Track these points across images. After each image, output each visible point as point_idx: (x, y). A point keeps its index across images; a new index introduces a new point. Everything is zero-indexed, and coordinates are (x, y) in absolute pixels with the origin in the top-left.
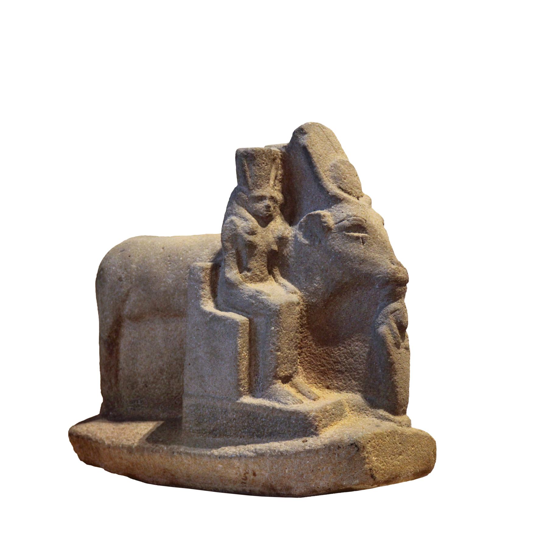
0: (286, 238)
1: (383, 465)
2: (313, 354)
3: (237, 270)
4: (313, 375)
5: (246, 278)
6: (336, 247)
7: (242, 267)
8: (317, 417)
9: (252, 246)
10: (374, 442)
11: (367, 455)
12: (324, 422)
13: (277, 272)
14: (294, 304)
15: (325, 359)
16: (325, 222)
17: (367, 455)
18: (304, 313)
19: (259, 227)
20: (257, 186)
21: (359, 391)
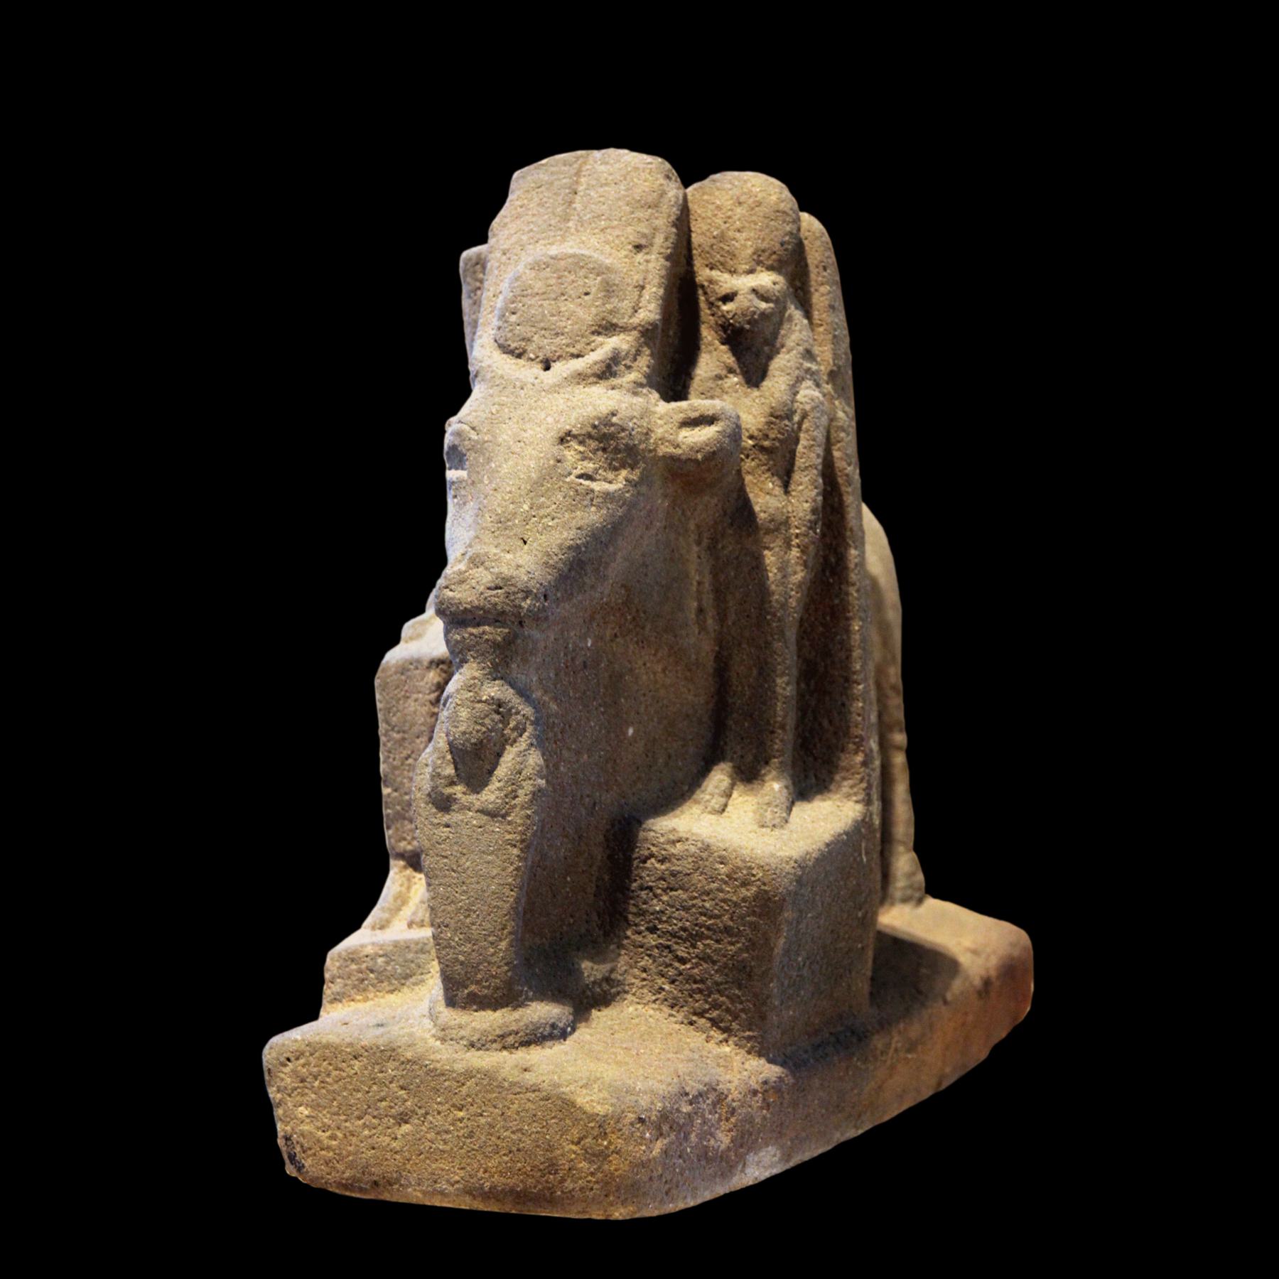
1: (333, 1137)
10: (303, 1066)
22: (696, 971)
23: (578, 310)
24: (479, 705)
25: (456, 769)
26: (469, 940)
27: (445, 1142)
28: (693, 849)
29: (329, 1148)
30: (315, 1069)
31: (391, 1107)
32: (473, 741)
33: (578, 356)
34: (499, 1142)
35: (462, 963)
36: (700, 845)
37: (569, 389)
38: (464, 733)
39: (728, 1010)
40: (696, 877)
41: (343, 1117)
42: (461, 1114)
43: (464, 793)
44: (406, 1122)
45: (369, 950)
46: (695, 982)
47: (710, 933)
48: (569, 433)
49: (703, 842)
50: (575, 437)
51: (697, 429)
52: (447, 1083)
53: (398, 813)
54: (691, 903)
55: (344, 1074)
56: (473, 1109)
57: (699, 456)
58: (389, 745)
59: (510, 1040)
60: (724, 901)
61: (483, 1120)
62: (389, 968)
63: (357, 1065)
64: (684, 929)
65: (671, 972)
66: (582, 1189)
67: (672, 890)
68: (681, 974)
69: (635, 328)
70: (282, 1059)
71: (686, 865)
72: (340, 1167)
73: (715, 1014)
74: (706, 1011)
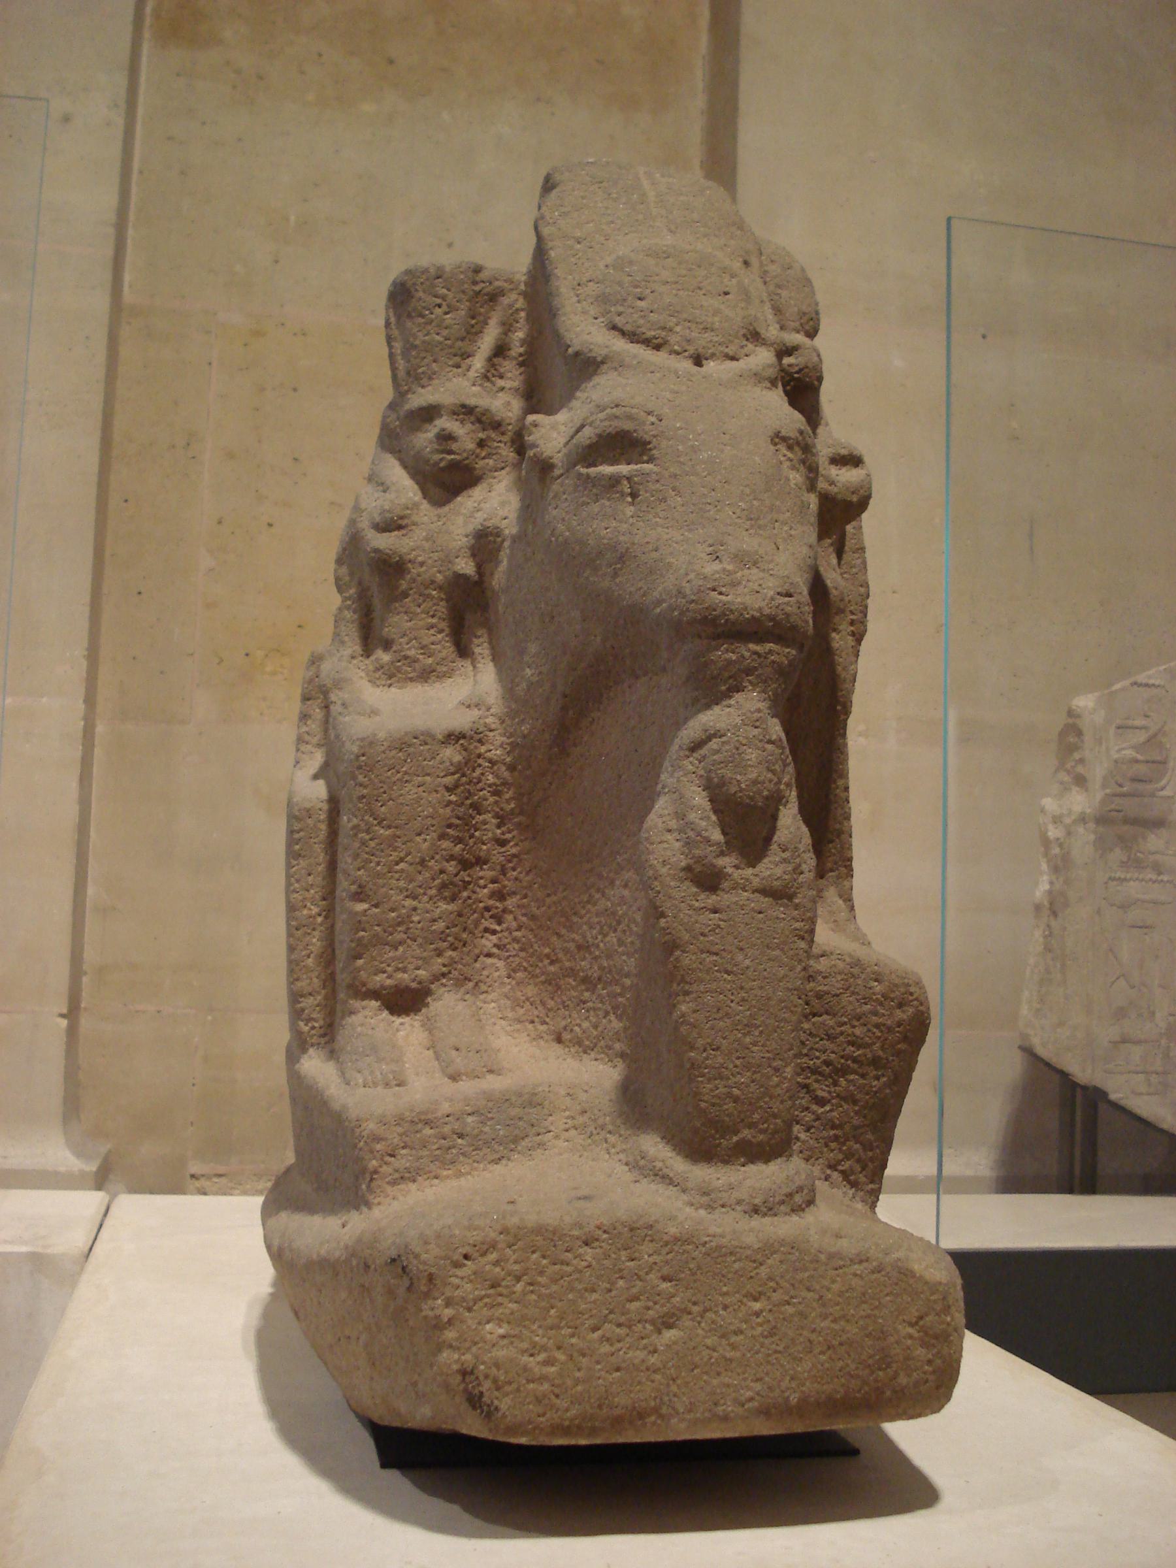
0: (497, 532)
1: (548, 1362)
2: (533, 918)
3: (358, 649)
4: (531, 990)
5: (377, 669)
6: (561, 527)
7: (370, 637)
8: (378, 1139)
9: (390, 569)
10: (496, 1263)
11: (448, 1312)
12: (404, 1160)
13: (481, 648)
14: (433, 737)
15: (559, 935)
16: (534, 446)
17: (448, 1312)
18: (506, 774)
19: (425, 505)
20: (418, 378)
21: (622, 1055)
22: (835, 1114)
23: (722, 307)
24: (769, 747)
25: (724, 833)
26: (747, 1067)
27: (734, 1347)
28: (841, 965)
29: (543, 1378)
30: (516, 1267)
31: (648, 1308)
32: (765, 793)
33: (733, 358)
34: (813, 1337)
35: (736, 1100)
36: (848, 960)
37: (749, 388)
38: (755, 782)
39: (858, 1161)
40: (845, 998)
41: (566, 1331)
42: (757, 1306)
43: (737, 867)
44: (670, 1326)
45: (446, 1107)
46: (833, 1127)
47: (855, 1066)
48: (777, 435)
49: (850, 956)
50: (784, 439)
51: (844, 469)
52: (737, 1266)
53: (376, 935)
54: (839, 1030)
55: (568, 1269)
56: (776, 1297)
57: (855, 499)
58: (372, 844)
59: (798, 1199)
60: (877, 1026)
61: (790, 1310)
62: (487, 1129)
63: (588, 1253)
64: (827, 1063)
65: (809, 1117)
66: (916, 1384)
67: (814, 1015)
68: (818, 1119)
69: (772, 345)
70: (457, 1256)
71: (835, 985)
72: (562, 1403)
73: (846, 1165)
74: (839, 1162)
